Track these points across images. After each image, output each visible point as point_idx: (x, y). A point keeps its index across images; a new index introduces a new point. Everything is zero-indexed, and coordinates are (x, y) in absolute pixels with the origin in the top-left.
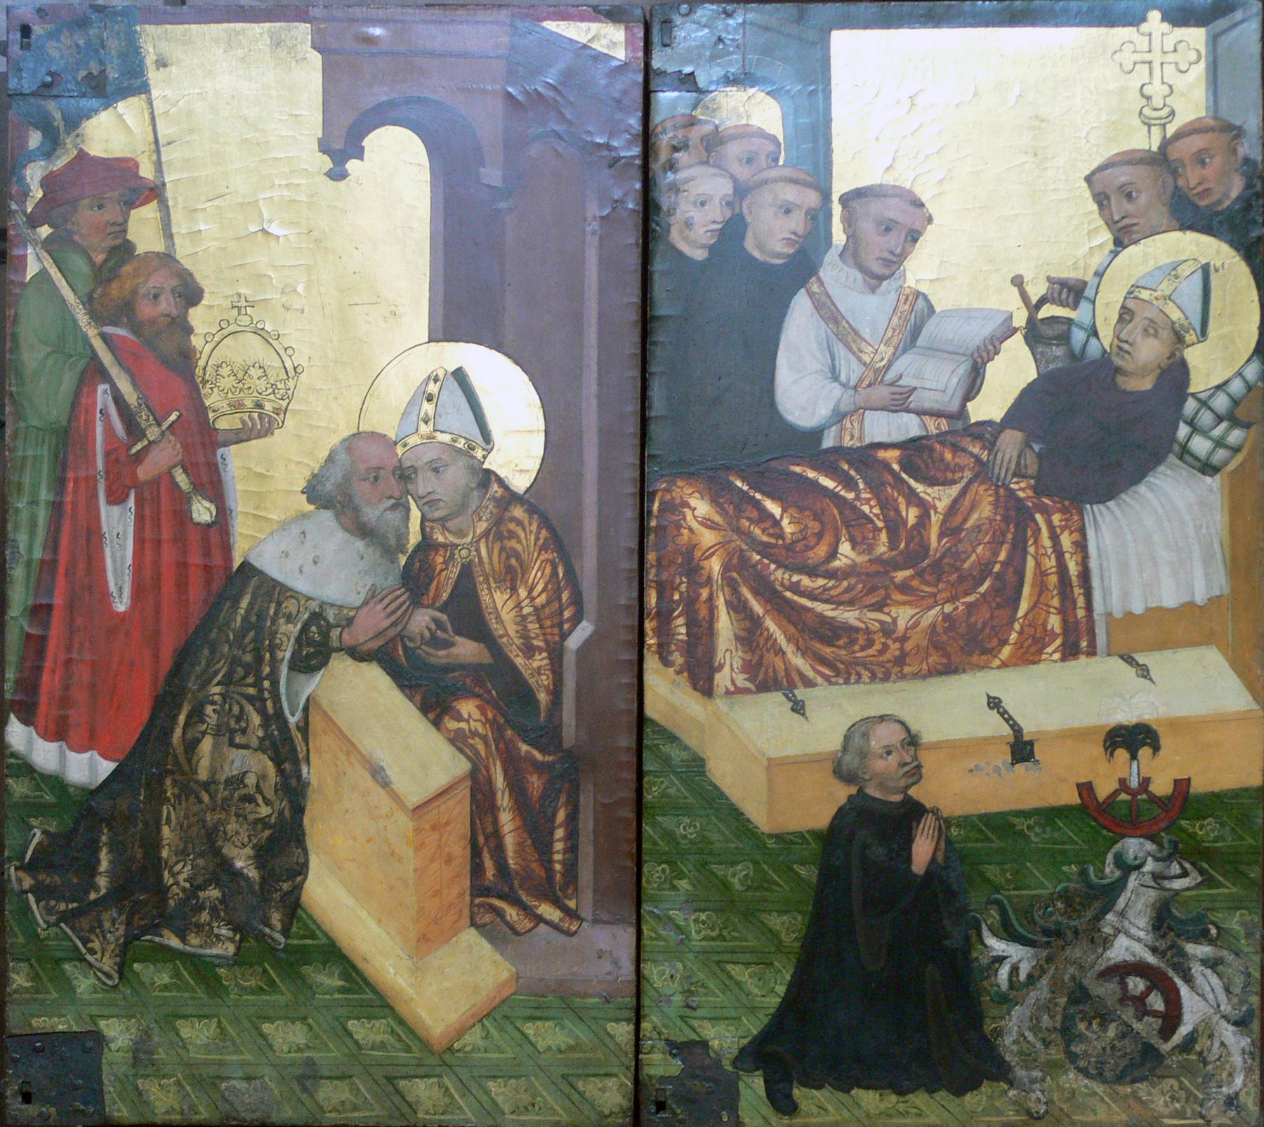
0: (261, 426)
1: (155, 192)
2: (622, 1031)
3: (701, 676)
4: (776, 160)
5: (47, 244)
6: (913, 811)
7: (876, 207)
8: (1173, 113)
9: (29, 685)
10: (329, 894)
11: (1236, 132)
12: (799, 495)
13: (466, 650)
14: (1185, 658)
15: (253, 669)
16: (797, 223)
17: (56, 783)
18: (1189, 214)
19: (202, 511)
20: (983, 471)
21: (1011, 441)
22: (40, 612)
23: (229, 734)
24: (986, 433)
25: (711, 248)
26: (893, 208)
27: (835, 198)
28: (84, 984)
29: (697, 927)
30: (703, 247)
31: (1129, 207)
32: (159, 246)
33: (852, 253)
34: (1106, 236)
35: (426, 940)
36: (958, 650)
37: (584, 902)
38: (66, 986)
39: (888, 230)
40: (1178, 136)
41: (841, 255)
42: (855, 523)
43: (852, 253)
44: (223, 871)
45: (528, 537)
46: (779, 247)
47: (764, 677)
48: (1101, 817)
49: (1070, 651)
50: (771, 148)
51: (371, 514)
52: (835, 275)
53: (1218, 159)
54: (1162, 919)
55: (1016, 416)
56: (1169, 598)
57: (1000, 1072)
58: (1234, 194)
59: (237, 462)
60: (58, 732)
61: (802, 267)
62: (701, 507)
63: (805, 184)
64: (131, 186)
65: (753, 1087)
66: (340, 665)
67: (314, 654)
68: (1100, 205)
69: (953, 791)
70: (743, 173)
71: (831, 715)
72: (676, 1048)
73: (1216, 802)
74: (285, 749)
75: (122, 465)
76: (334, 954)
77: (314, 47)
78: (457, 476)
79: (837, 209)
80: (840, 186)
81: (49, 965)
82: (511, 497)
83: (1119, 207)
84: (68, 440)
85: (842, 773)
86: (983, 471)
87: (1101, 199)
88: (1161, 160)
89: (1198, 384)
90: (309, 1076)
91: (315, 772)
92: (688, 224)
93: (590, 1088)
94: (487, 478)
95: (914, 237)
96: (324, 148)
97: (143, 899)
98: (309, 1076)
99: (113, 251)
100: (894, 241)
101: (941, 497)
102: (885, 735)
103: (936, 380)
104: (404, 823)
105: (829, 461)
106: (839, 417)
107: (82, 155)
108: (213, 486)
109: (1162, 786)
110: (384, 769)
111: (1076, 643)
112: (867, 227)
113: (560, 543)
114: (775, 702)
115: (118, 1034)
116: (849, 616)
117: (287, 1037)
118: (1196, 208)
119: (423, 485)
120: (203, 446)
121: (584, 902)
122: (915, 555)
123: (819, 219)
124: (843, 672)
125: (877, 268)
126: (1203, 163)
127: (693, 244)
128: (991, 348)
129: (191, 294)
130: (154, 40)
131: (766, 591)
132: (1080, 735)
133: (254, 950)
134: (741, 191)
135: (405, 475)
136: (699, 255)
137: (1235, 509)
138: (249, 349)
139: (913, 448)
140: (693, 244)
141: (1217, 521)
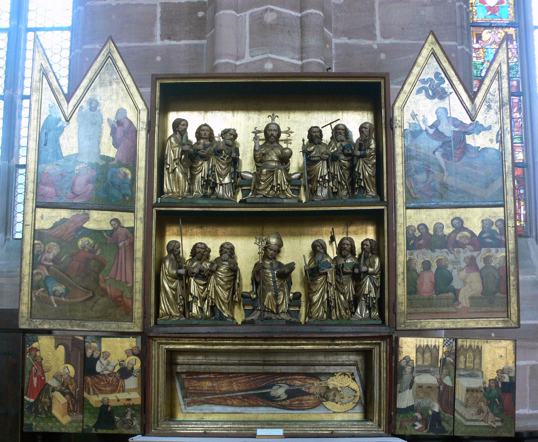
0: (49, 371)
2: (81, 424)
3: (89, 393)
6: (108, 406)
9: (27, 393)
10: (55, 412)
11: (138, 347)
12: (97, 378)
13: (67, 391)
14: (134, 393)
15: (47, 392)
16: (98, 354)
17: (29, 401)
18: (134, 354)
19: (43, 378)
20: (115, 376)
21: (118, 374)
22: (28, 387)
23: (45, 398)
24: (115, 373)
26: (107, 354)
28: (31, 419)
29: (88, 415)
33: (103, 357)
35: (63, 416)
36: (112, 392)
37: (78, 413)
38: (29, 419)
42: (103, 381)
43: (103, 357)
44: (44, 410)
45: (73, 381)
47: (95, 394)
48: (126, 406)
49: (123, 392)
51: (59, 379)
52: (101, 359)
54: (131, 415)
55: (118, 371)
56: (132, 388)
57: (117, 428)
59: (46, 374)
60: (29, 397)
61: (98, 358)
64: (37, 350)
65: (94, 429)
66: (56, 392)
67: (53, 390)
69: (112, 404)
71: (101, 397)
72: (87, 426)
73: (136, 405)
74: (50, 399)
76: (54, 417)
78: (67, 376)
81: (28, 417)
82: (71, 378)
84: (31, 372)
85: (102, 402)
86: (115, 376)
89: (135, 369)
90: (52, 428)
91: (53, 401)
93: (78, 429)
94: (69, 376)
97: (37, 412)
98: (52, 428)
101: (111, 378)
102: (106, 399)
103: (111, 368)
104: (61, 406)
105: (101, 375)
106: (102, 371)
108: (44, 376)
109: (131, 404)
110: (59, 401)
111: (123, 391)
114: (96, 396)
115: (34, 424)
116: (103, 388)
117: (50, 424)
119: (64, 376)
120: (43, 372)
121: (78, 413)
122: (109, 383)
123: (100, 354)
124: (102, 393)
128: (116, 366)
129: (42, 359)
131: (95, 387)
132: (124, 399)
133: (47, 416)
135: (62, 375)
137: (138, 380)
139: (108, 374)
141: (137, 381)
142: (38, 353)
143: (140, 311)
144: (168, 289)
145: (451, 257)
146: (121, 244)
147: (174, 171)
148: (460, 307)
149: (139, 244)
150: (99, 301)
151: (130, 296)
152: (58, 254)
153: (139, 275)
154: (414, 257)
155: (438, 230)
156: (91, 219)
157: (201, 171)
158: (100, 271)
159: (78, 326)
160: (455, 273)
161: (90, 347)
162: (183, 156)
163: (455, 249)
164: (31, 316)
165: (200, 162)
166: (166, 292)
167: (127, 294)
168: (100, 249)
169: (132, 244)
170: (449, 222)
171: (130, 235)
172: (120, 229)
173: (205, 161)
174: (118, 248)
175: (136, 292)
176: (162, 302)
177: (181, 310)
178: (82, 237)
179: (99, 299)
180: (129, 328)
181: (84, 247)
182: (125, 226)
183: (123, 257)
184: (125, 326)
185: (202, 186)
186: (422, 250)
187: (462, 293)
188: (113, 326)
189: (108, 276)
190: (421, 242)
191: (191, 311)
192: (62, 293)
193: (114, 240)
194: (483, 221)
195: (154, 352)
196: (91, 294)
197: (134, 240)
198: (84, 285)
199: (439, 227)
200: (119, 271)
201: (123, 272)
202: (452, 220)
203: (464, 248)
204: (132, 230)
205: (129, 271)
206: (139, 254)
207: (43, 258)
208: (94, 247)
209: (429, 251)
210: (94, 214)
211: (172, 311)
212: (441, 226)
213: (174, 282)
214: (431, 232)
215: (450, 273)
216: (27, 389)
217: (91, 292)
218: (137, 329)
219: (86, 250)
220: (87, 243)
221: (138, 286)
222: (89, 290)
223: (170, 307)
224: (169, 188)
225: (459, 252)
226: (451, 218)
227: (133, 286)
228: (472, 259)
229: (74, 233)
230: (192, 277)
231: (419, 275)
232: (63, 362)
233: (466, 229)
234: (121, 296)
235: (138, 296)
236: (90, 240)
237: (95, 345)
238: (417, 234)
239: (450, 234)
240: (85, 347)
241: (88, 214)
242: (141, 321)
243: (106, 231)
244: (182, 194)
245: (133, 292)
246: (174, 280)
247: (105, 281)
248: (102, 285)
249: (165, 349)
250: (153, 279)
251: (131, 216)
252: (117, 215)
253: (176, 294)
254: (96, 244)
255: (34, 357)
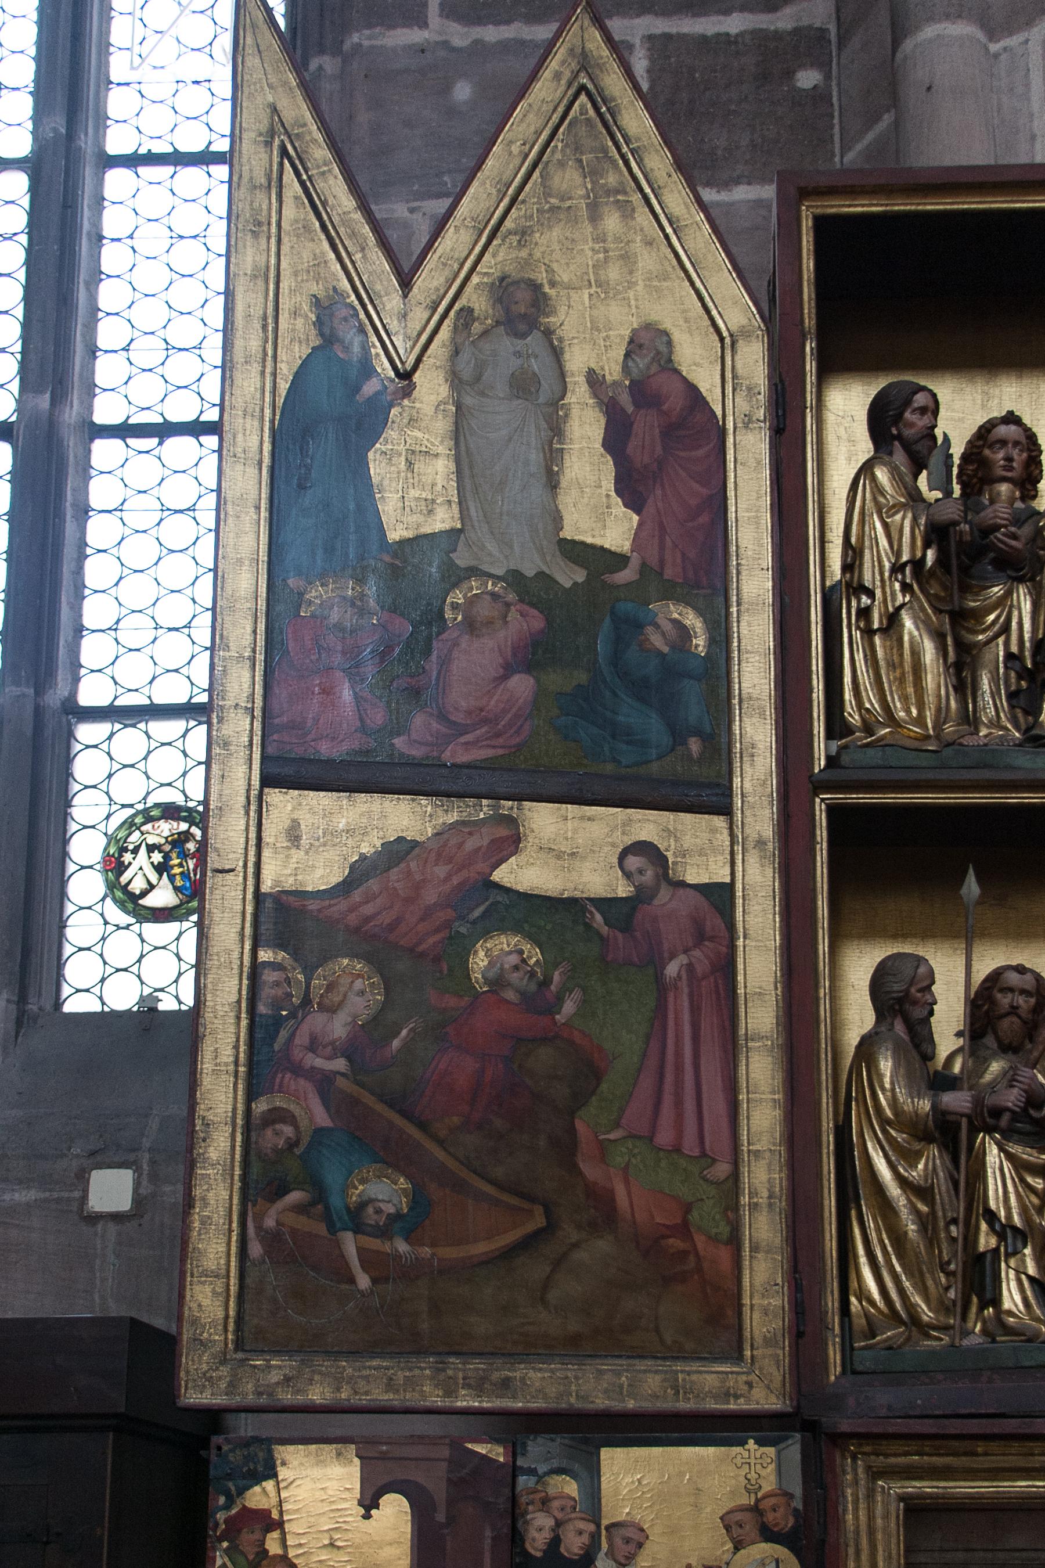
1: (280, 1525)
4: (575, 1508)
5: (227, 1551)
7: (623, 1532)
8: (760, 1487)
25: (544, 1551)
27: (603, 1527)
30: (540, 1550)
31: (740, 1531)
32: (280, 1552)
33: (611, 1554)
34: (729, 1546)
39: (628, 1542)
40: (764, 1497)
41: (606, 1554)
46: (576, 1551)
50: (572, 1503)
53: (782, 1509)
58: (790, 1525)
63: (589, 1521)
68: (727, 1530)
70: (560, 1516)
77: (357, 1456)
79: (604, 1532)
80: (605, 1522)
83: (736, 1531)
87: (728, 1528)
88: (756, 1509)
92: (534, 1540)
95: (640, 1545)
96: (360, 1503)
99: (257, 1554)
100: (631, 1548)
107: (244, 1506)
112: (618, 1541)
118: (772, 1531)
123: (595, 1537)
125: (623, 1561)
126: (775, 1510)
127: (536, 1549)
130: (285, 1452)
134: (559, 1524)
136: (539, 1554)
140: (536, 1549)
142: (273, 1546)
143: (778, 1301)
144: (894, 1190)
146: (672, 969)
147: (893, 620)
149: (759, 967)
150: (581, 1255)
151: (724, 1230)
152: (375, 1020)
153: (763, 1119)
156: (530, 844)
157: (1006, 629)
158: (579, 1099)
159: (479, 1387)
161: (545, 1501)
162: (931, 555)
164: (248, 1337)
165: (997, 590)
166: (885, 1207)
167: (707, 1215)
168: (577, 994)
169: (726, 967)
171: (714, 923)
172: (664, 894)
173: (1021, 580)
174: (662, 988)
175: (754, 1207)
176: (863, 1260)
177: (952, 1294)
178: (486, 934)
179: (576, 1246)
180: (728, 1395)
181: (497, 982)
182: (692, 878)
183: (687, 1029)
184: (708, 1384)
185: (1011, 696)
188: (646, 1386)
189: (617, 1125)
191: (996, 1301)
192: (397, 1217)
193: (646, 945)
195: (853, 1515)
196: (539, 1221)
197: (733, 947)
198: (499, 1172)
200: (668, 1099)
201: (689, 1105)
204: (721, 897)
205: (715, 1104)
206: (761, 1017)
207: (302, 1038)
208: (546, 982)
210: (543, 820)
211: (917, 1299)
213: (918, 1155)
217: (538, 1210)
218: (765, 1399)
219: (510, 995)
220: (514, 959)
221: (763, 1176)
222: (531, 1199)
223: (907, 1284)
224: (872, 701)
227: (735, 1176)
229: (450, 913)
230: (989, 1130)
234: (684, 1229)
235: (764, 1229)
236: (527, 947)
237: (571, 1488)
240: (514, 1499)
241: (511, 821)
242: (784, 1352)
243: (604, 904)
244: (938, 725)
245: (736, 1207)
246: (917, 1146)
247: (603, 1150)
248: (590, 1171)
249: (902, 1498)
250: (829, 1139)
251: (714, 831)
252: (647, 825)
253: (933, 1212)
254: (556, 966)
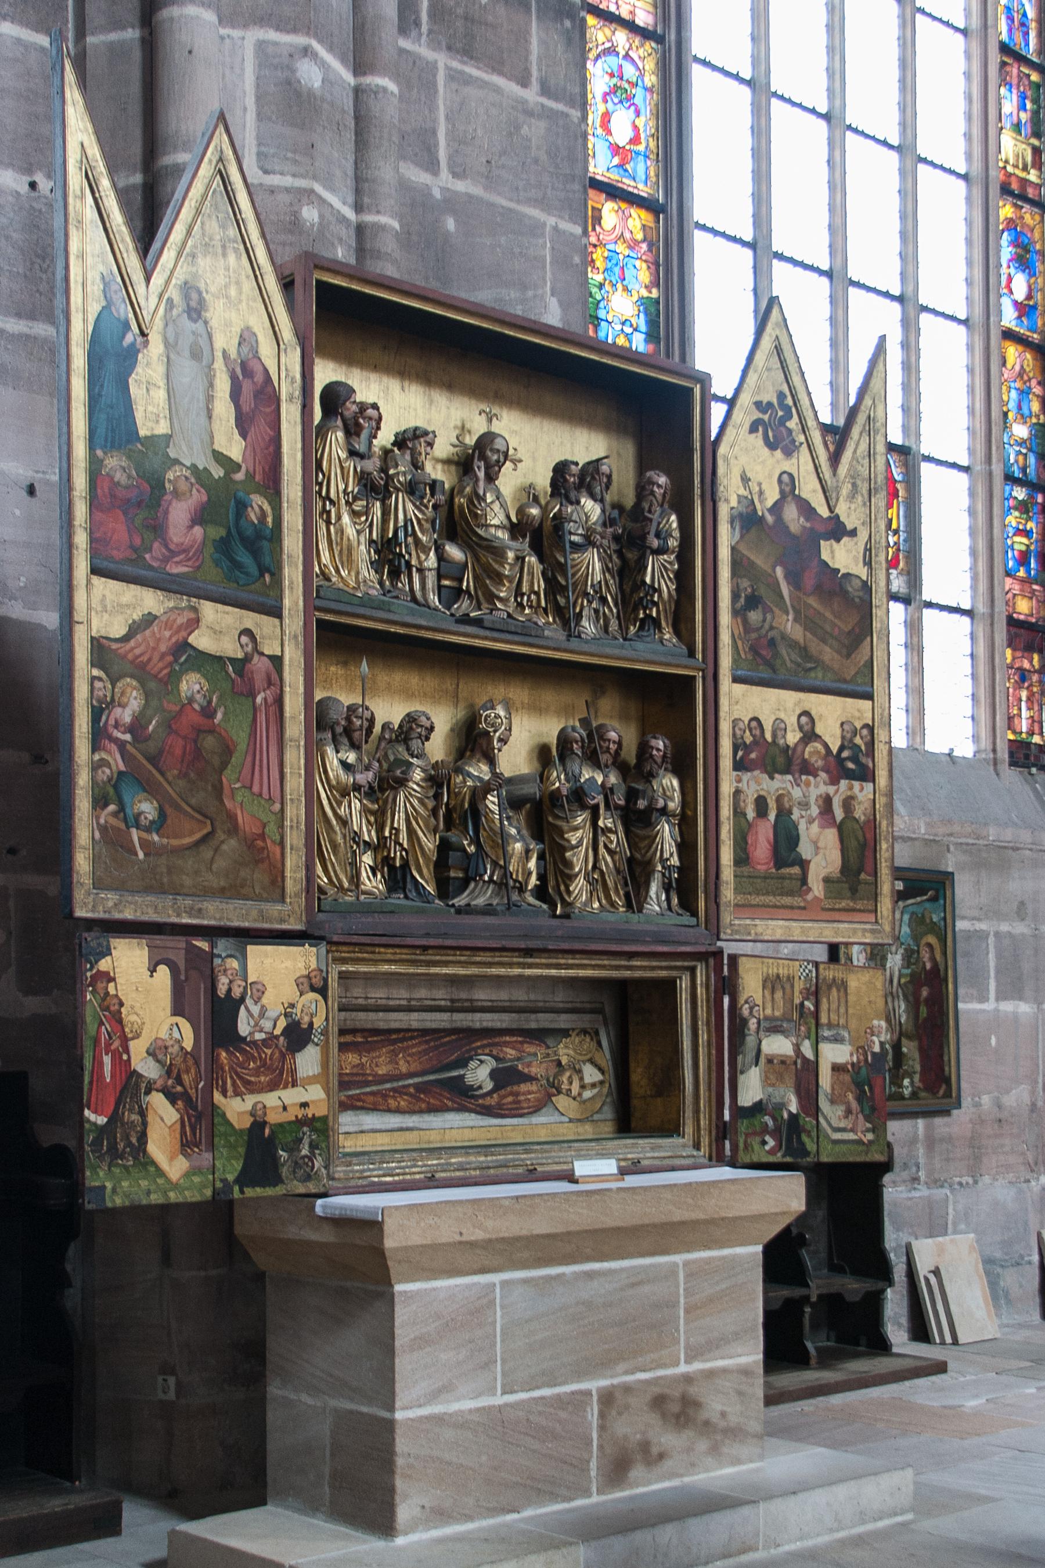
0: (137, 1036)
1: (113, 979)
19: (125, 1057)
59: (132, 1044)
62: (224, 1054)
75: (108, 1045)
78: (176, 1047)
82: (187, 1053)
94: (182, 1048)
108: (127, 1051)
113: (197, 1063)
120: (125, 1041)
135: (166, 1048)
138: (133, 1018)
145: (797, 793)
148: (809, 897)
154: (743, 786)
155: (780, 733)
160: (802, 826)
163: (804, 777)
170: (794, 719)
186: (757, 773)
187: (812, 866)
190: (753, 756)
194: (842, 724)
199: (780, 727)
202: (800, 716)
203: (815, 776)
209: (766, 776)
212: (782, 726)
214: (769, 737)
215: (796, 828)
216: (90, 1090)
225: (808, 784)
226: (798, 712)
228: (827, 802)
231: (750, 825)
232: (168, 1011)
233: (818, 737)
238: (748, 739)
239: (796, 745)
240: (212, 970)
255: (104, 999)
